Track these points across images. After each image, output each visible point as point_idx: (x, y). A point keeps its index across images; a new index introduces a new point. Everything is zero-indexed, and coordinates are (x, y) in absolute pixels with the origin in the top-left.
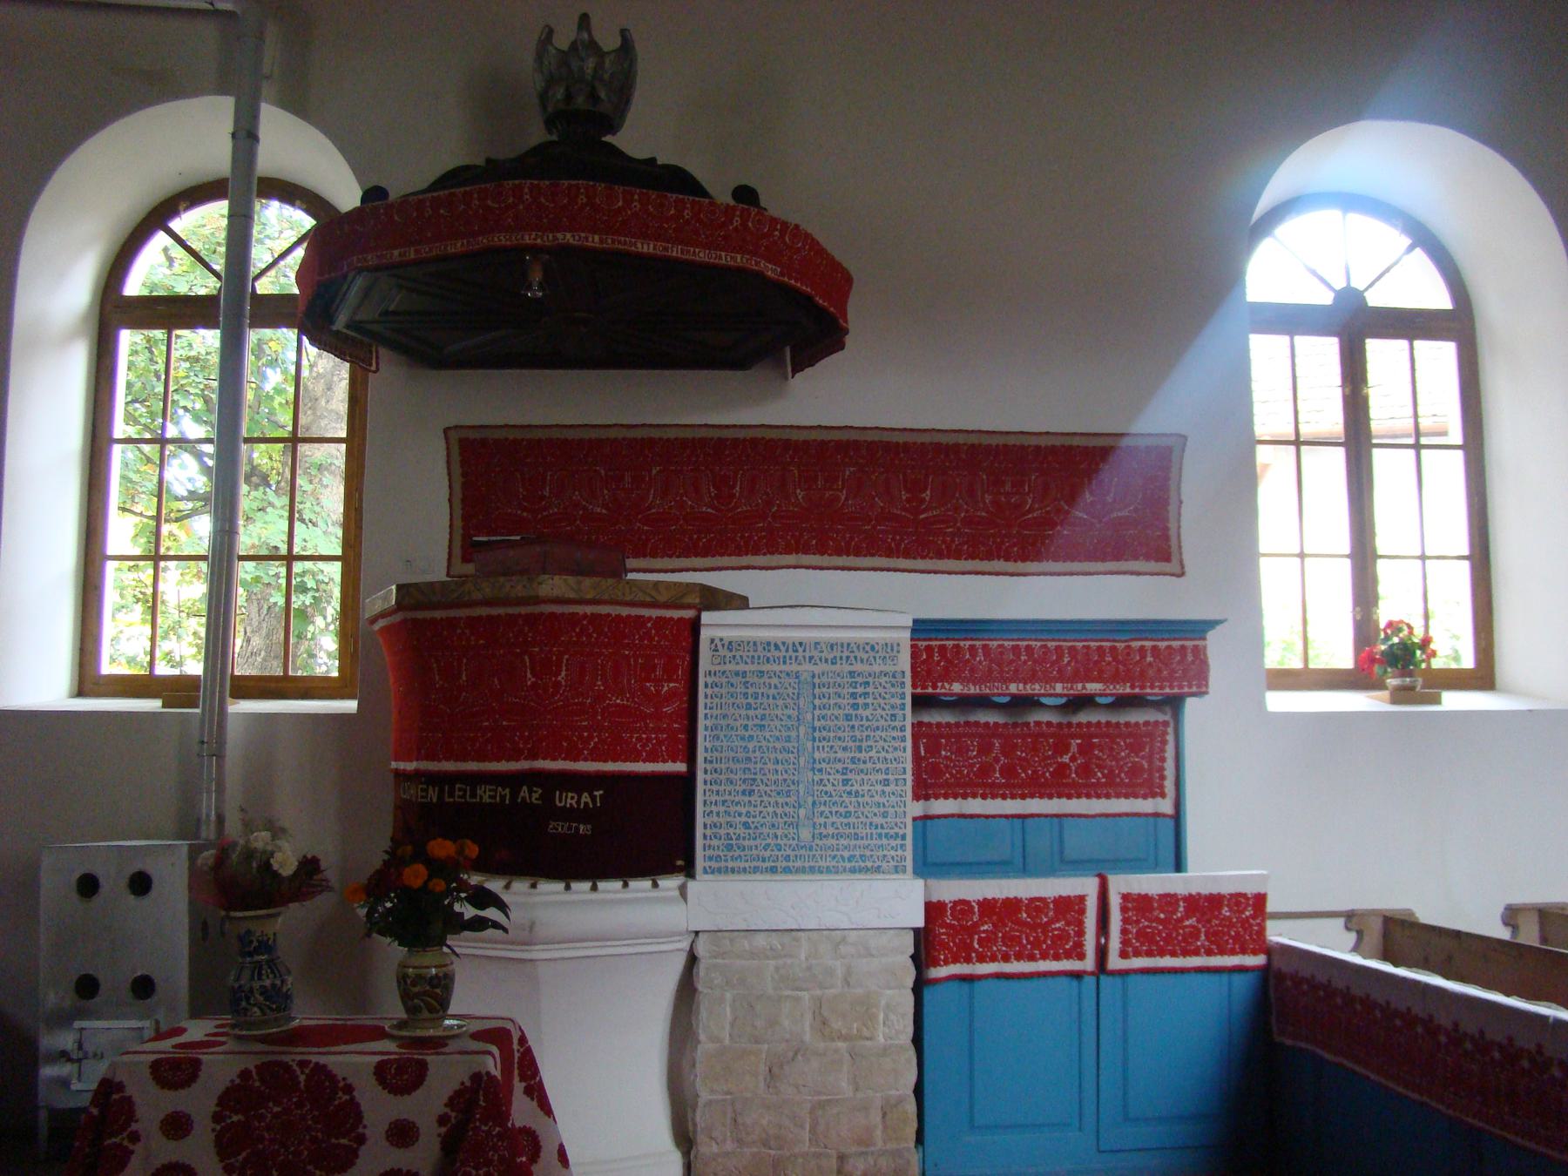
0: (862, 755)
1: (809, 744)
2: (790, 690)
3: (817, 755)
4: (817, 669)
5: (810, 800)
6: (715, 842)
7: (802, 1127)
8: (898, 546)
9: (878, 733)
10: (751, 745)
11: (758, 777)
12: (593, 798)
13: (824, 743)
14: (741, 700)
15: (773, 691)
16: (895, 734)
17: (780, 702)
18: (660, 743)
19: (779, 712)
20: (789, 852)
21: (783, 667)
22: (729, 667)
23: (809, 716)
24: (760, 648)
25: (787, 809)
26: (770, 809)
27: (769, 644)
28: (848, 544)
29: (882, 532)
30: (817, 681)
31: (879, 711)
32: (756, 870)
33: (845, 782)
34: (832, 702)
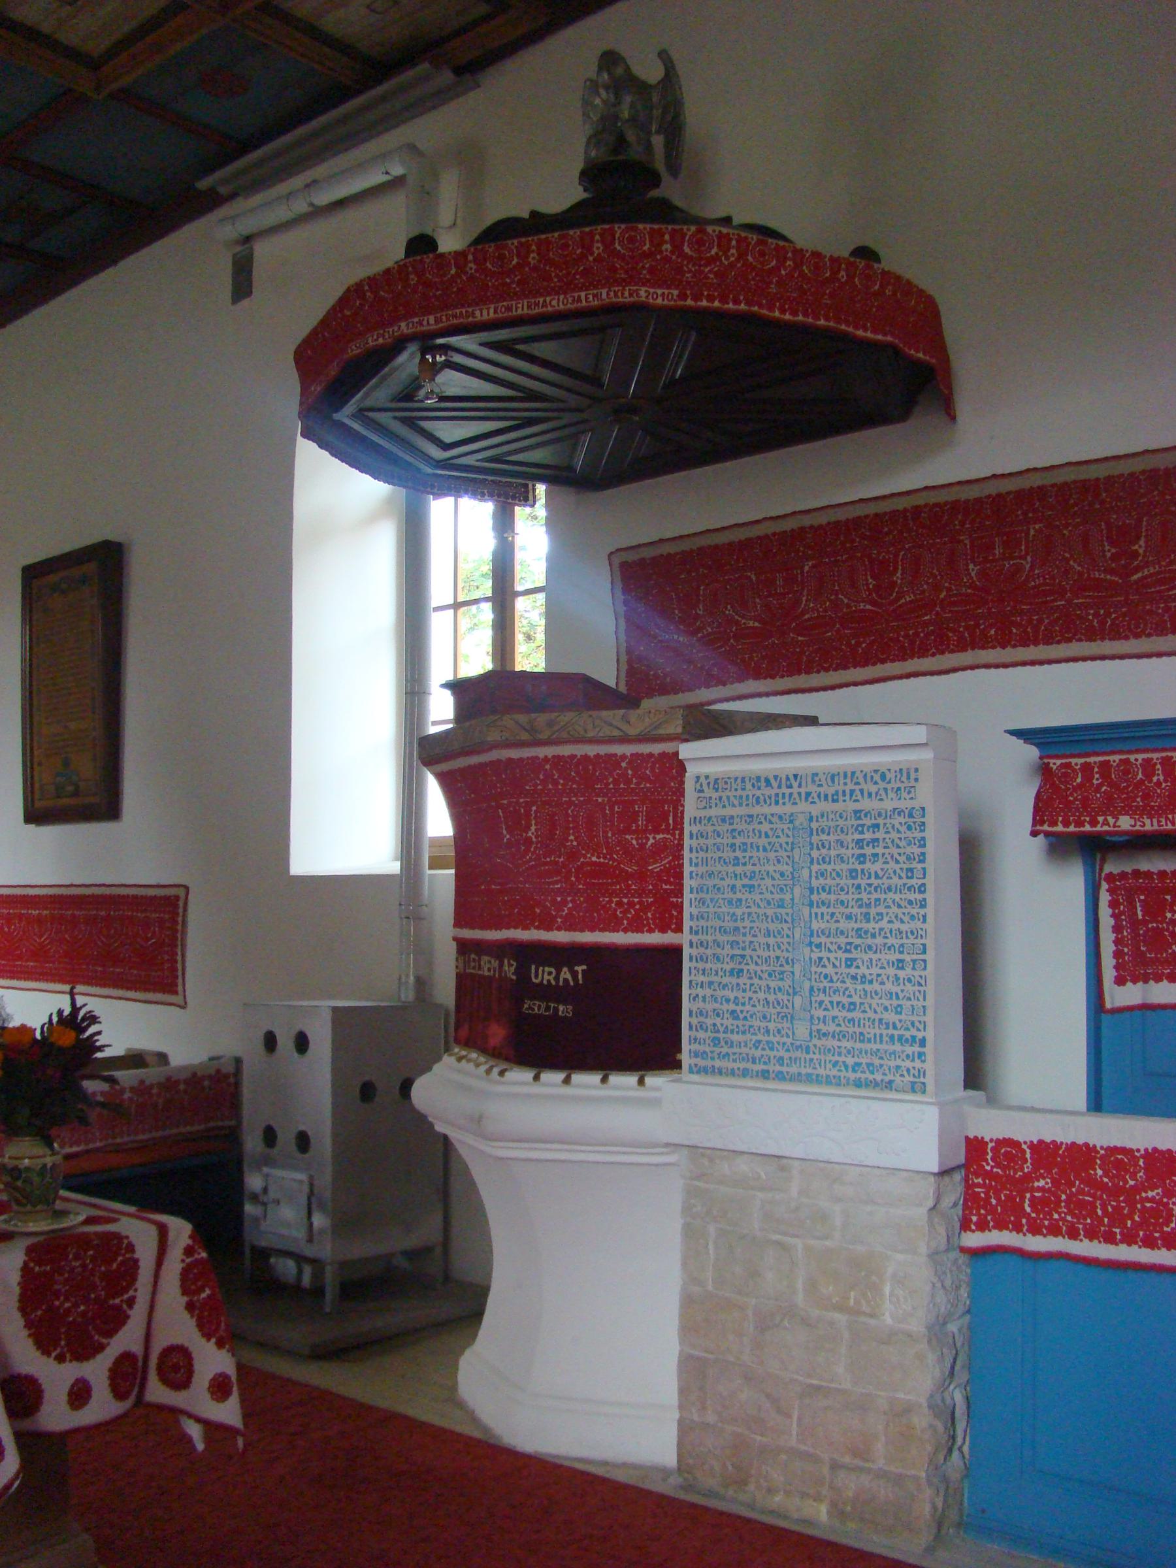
0: (871, 926)
2: (783, 840)
4: (815, 810)
5: (807, 985)
6: (701, 1035)
7: (788, 1416)
8: (1102, 623)
9: (891, 895)
10: (739, 912)
11: (748, 952)
12: (574, 974)
13: (824, 909)
14: (728, 854)
15: (763, 841)
16: (912, 896)
17: (772, 855)
18: (645, 908)
19: (771, 869)
20: (782, 1053)
22: (713, 812)
23: (805, 873)
24: (749, 786)
25: (780, 996)
26: (761, 995)
27: (758, 779)
29: (1079, 606)
30: (814, 825)
31: (892, 864)
32: (745, 1073)
33: (850, 962)
34: (833, 853)
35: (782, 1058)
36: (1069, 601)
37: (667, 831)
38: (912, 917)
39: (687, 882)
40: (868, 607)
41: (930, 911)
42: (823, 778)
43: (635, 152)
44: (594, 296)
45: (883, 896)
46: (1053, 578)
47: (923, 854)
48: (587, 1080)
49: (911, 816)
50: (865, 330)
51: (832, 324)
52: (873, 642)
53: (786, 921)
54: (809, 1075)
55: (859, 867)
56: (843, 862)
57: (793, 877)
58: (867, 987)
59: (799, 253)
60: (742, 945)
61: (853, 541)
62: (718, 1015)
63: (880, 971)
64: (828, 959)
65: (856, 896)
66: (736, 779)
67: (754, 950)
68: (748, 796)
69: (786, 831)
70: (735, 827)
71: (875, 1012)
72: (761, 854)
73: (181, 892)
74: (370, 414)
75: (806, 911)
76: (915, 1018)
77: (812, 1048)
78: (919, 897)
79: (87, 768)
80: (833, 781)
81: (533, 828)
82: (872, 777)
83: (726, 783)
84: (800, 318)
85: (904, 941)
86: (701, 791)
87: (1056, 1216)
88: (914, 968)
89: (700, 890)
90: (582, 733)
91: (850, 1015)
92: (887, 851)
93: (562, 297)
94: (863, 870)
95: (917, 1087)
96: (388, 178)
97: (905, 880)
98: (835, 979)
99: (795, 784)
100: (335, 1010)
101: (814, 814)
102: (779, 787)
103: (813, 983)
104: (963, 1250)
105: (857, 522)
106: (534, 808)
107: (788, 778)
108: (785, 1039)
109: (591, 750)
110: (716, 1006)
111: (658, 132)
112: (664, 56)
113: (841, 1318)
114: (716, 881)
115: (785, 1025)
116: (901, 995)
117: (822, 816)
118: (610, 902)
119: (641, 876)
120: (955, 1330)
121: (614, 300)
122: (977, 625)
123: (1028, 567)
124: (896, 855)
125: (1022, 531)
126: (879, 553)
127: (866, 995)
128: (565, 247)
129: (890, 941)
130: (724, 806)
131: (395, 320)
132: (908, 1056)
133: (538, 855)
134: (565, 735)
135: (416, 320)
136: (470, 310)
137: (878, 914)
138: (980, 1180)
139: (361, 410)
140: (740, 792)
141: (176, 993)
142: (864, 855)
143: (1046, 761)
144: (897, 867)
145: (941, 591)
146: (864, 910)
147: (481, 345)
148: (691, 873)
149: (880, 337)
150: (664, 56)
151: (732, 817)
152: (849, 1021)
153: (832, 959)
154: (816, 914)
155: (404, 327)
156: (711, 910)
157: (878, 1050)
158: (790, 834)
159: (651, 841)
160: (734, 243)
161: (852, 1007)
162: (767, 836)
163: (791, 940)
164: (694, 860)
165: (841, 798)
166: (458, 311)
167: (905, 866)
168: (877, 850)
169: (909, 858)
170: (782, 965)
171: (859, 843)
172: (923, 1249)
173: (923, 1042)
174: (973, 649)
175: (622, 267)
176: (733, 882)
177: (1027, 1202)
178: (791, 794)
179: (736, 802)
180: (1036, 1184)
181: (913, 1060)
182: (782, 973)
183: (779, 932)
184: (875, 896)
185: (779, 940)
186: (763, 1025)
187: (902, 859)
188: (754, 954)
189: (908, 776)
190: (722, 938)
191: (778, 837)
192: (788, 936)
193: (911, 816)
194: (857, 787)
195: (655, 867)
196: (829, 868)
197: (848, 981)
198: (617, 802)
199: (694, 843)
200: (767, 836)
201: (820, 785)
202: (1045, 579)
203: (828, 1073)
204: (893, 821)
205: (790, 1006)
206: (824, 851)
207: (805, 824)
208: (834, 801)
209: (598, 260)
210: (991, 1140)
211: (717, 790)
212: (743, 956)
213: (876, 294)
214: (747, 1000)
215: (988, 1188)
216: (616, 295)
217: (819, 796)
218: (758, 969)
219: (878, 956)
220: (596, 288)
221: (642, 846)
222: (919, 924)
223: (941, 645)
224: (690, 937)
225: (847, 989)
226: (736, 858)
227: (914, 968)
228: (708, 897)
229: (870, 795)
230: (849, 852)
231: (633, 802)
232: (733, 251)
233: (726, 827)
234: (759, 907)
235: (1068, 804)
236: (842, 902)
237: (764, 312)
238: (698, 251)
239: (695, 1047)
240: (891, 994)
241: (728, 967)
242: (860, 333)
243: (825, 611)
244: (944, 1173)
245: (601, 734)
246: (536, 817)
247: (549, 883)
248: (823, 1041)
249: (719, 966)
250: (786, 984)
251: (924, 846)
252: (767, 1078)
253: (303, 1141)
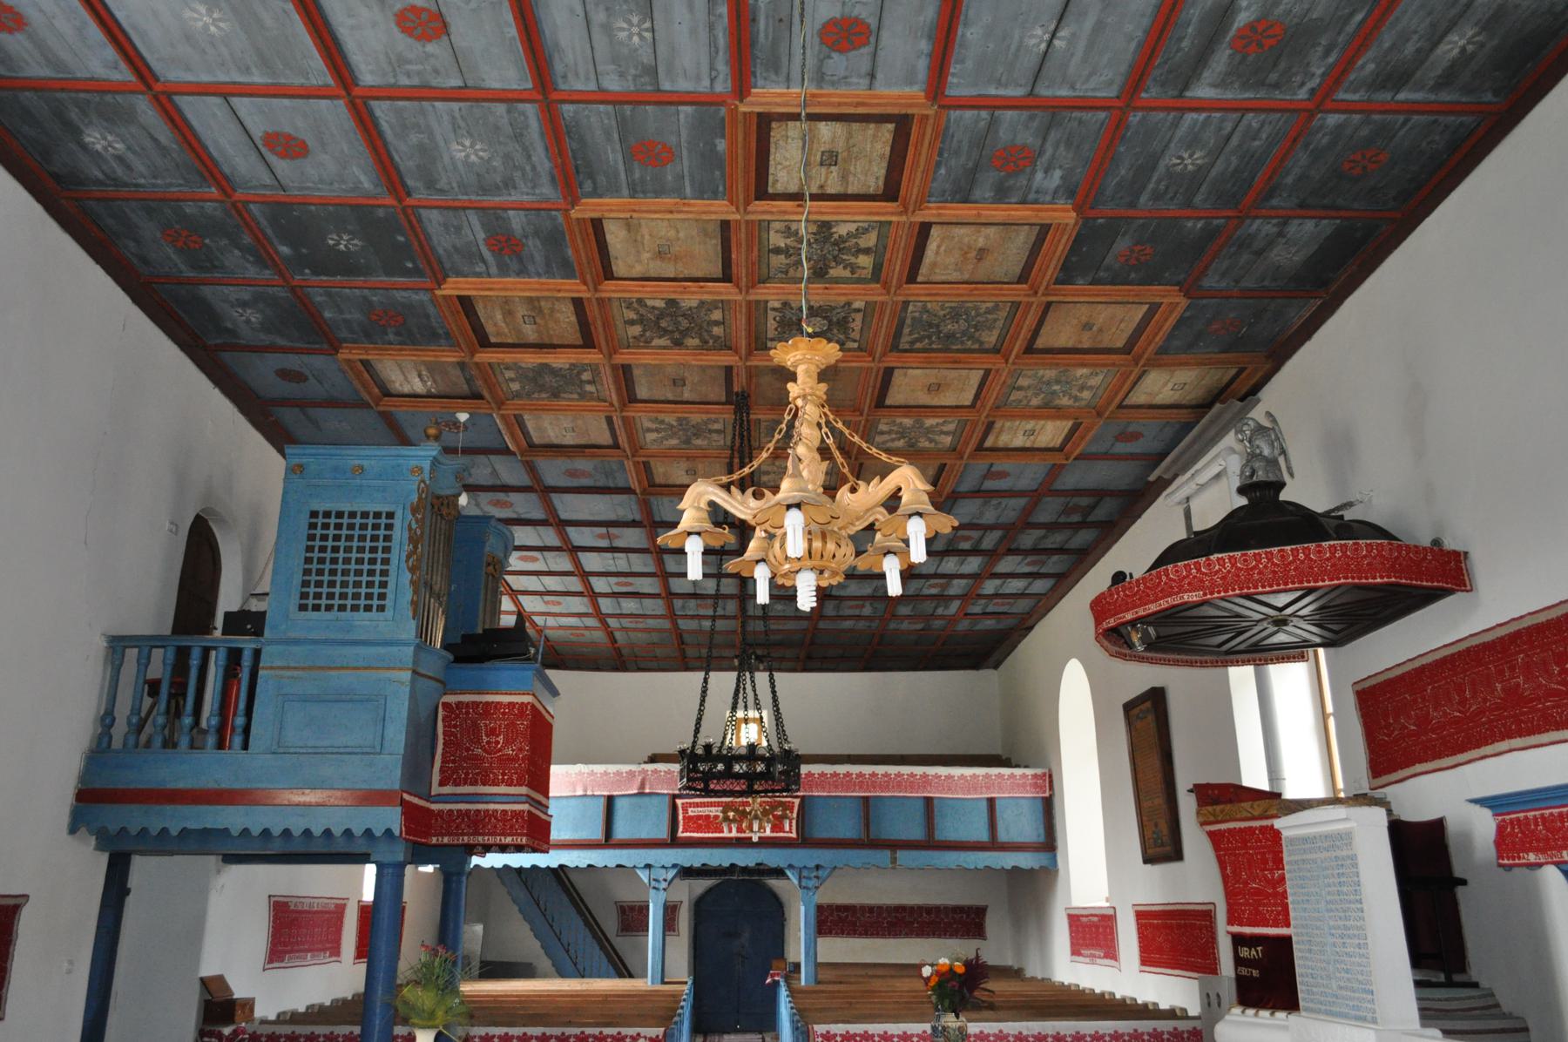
48: (1265, 1013)
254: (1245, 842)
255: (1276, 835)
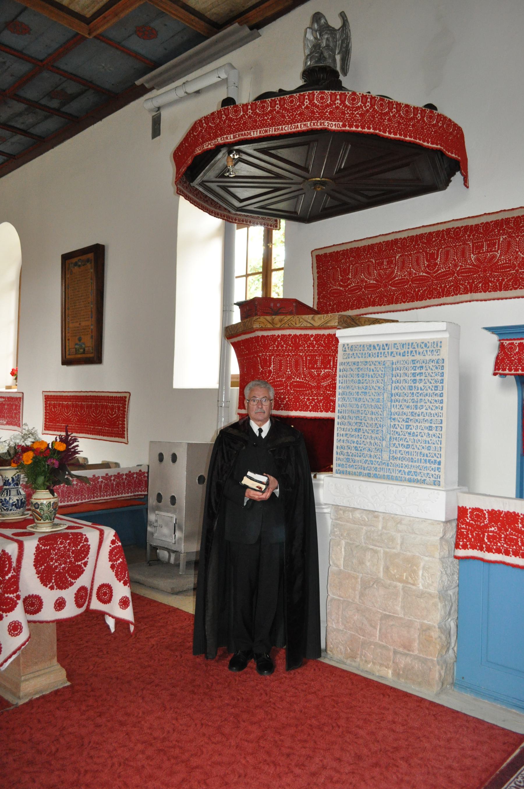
1: (389, 404)
3: (393, 410)
4: (395, 360)
5: (388, 436)
6: (341, 457)
9: (427, 397)
10: (360, 404)
11: (363, 421)
13: (397, 403)
14: (356, 379)
15: (372, 373)
16: (437, 398)
17: (375, 379)
19: (374, 385)
20: (377, 466)
21: (377, 359)
22: (350, 360)
23: (389, 387)
24: (366, 349)
25: (376, 441)
26: (368, 440)
27: (370, 346)
28: (501, 284)
30: (394, 366)
31: (428, 384)
32: (360, 474)
33: (408, 427)
34: (402, 378)
35: (376, 468)
36: (517, 271)
37: (330, 368)
38: (437, 408)
39: (338, 391)
40: (424, 274)
41: (444, 405)
42: (399, 346)
43: (329, 62)
44: (304, 125)
45: (423, 398)
46: (510, 260)
47: (443, 380)
49: (437, 362)
50: (428, 143)
51: (412, 139)
52: (425, 290)
53: (380, 408)
54: (388, 476)
55: (413, 385)
56: (406, 382)
57: (384, 389)
58: (416, 438)
59: (399, 105)
60: (360, 418)
61: (419, 245)
62: (349, 448)
63: (422, 431)
64: (398, 425)
65: (411, 398)
66: (360, 346)
67: (366, 420)
68: (365, 353)
69: (382, 369)
70: (359, 366)
71: (419, 449)
72: (370, 379)
73: (127, 395)
74: (207, 184)
75: (389, 404)
76: (436, 452)
77: (390, 464)
78: (440, 398)
79: (88, 342)
80: (403, 347)
81: (272, 366)
82: (421, 345)
83: (356, 347)
84: (398, 136)
85: (433, 418)
86: (346, 351)
87: (499, 544)
88: (436, 430)
89: (343, 393)
90: (294, 324)
91: (407, 450)
92: (426, 378)
93: (290, 125)
94: (415, 387)
95: (436, 483)
96: (219, 79)
97: (434, 391)
98: (401, 433)
99: (386, 348)
100: (188, 444)
101: (394, 361)
102: (379, 349)
103: (391, 435)
104: (456, 557)
105: (421, 236)
106: (273, 357)
107: (383, 345)
108: (378, 460)
109: (298, 332)
110: (349, 444)
111: (339, 53)
112: (343, 15)
113: (400, 585)
114: (350, 390)
115: (378, 453)
116: (430, 442)
117: (398, 362)
118: (304, 398)
119: (318, 387)
120: (451, 594)
121: (313, 127)
122: (473, 282)
123: (498, 255)
124: (430, 380)
125: (497, 239)
126: (430, 251)
127: (414, 441)
128: (292, 102)
129: (426, 418)
130: (355, 358)
131: (216, 137)
132: (432, 469)
133: (274, 377)
134: (287, 326)
135: (225, 136)
136: (249, 132)
137: (421, 406)
138: (464, 526)
139: (203, 181)
140: (362, 351)
141: (124, 438)
142: (415, 380)
143: (502, 341)
144: (430, 385)
145: (457, 267)
146: (415, 404)
147: (254, 150)
148: (340, 386)
149: (435, 146)
150: (343, 15)
151: (358, 362)
152: (407, 453)
153: (400, 425)
154: (394, 405)
155: (220, 140)
156: (348, 403)
157: (419, 466)
158: (383, 370)
159: (323, 372)
160: (369, 100)
161: (408, 446)
162: (373, 371)
163: (382, 416)
164: (341, 381)
165: (406, 355)
166: (243, 132)
167: (434, 385)
168: (422, 378)
169: (436, 382)
170: (378, 427)
171: (414, 374)
172: (437, 555)
173: (439, 463)
174: (471, 293)
175: (317, 112)
176: (357, 391)
177: (486, 537)
178: (384, 353)
179: (360, 356)
180: (490, 529)
181: (435, 471)
182: (378, 431)
183: (377, 413)
184: (419, 398)
185: (377, 416)
186: (369, 453)
187: (433, 382)
188: (366, 422)
189: (437, 345)
190: (351, 415)
191: (378, 371)
192: (381, 415)
193: (437, 362)
194: (414, 350)
195: (324, 384)
196: (400, 385)
197: (407, 435)
198: (308, 355)
199: (341, 373)
200: (373, 371)
201: (397, 349)
202: (506, 261)
203: (397, 475)
204: (429, 365)
205: (381, 445)
206: (398, 378)
207: (390, 366)
208: (403, 356)
209: (307, 107)
210: (470, 508)
211: (352, 351)
212: (361, 423)
213: (434, 126)
214: (362, 442)
215: (468, 530)
216: (314, 125)
217: (397, 353)
218: (367, 428)
219: (421, 424)
220: (305, 121)
221: (319, 375)
222: (440, 411)
223: (457, 291)
224: (338, 414)
225: (406, 438)
226: (359, 380)
227: (436, 430)
228: (346, 397)
229: (419, 353)
230: (409, 378)
231: (316, 355)
232: (368, 104)
233: (356, 366)
234: (369, 402)
235: (511, 361)
236: (405, 400)
237: (382, 133)
238: (353, 104)
239: (339, 462)
240: (426, 441)
241: (354, 428)
242: (425, 144)
243: (405, 276)
244: (447, 522)
245: (302, 325)
246: (273, 362)
247: (278, 390)
248: (395, 461)
249: (350, 427)
250: (379, 436)
251: (443, 376)
252: (370, 477)
253: (173, 500)
254: (296, 346)
255: (333, 340)
